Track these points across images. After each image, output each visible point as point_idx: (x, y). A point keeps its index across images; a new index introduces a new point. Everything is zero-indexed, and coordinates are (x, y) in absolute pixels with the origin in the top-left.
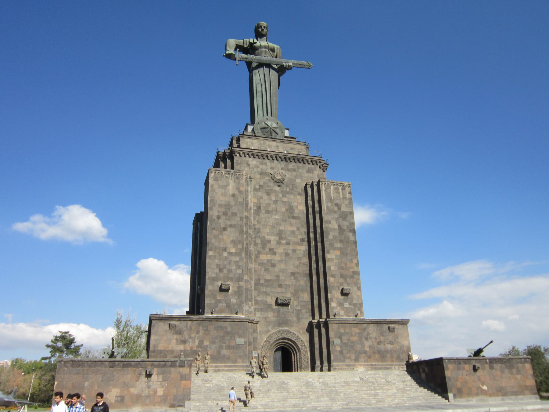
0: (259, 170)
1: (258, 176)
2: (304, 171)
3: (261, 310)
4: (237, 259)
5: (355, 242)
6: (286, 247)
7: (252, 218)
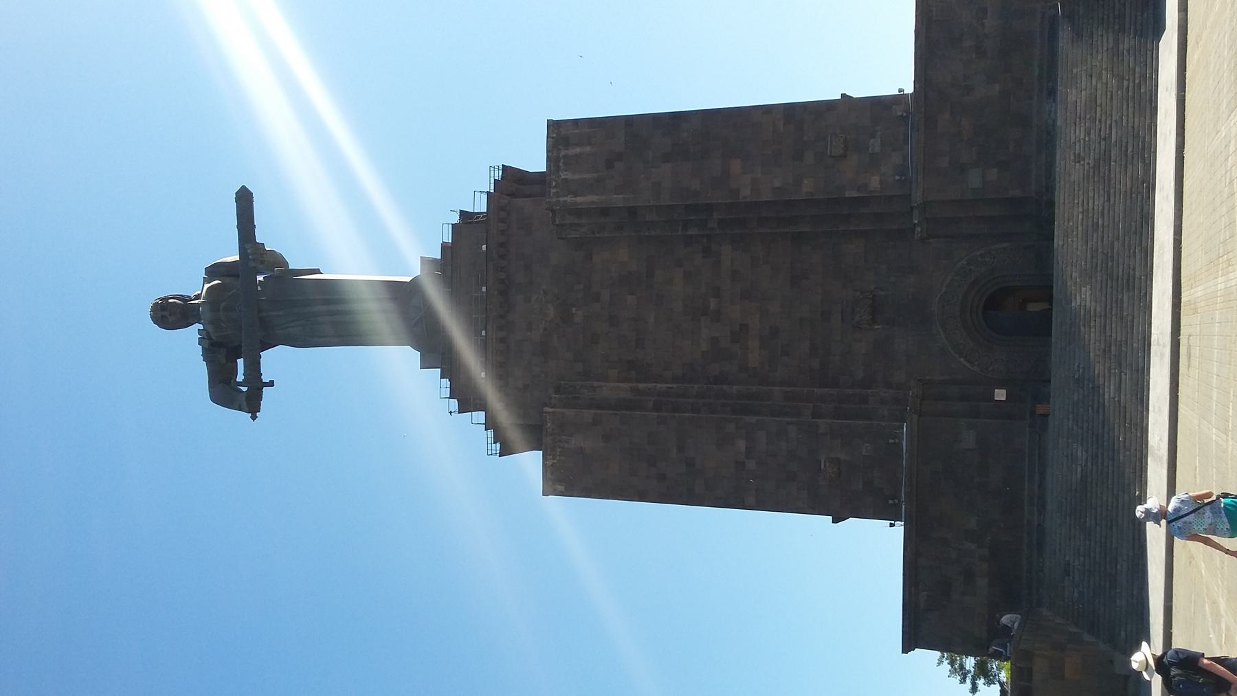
7: (661, 386)
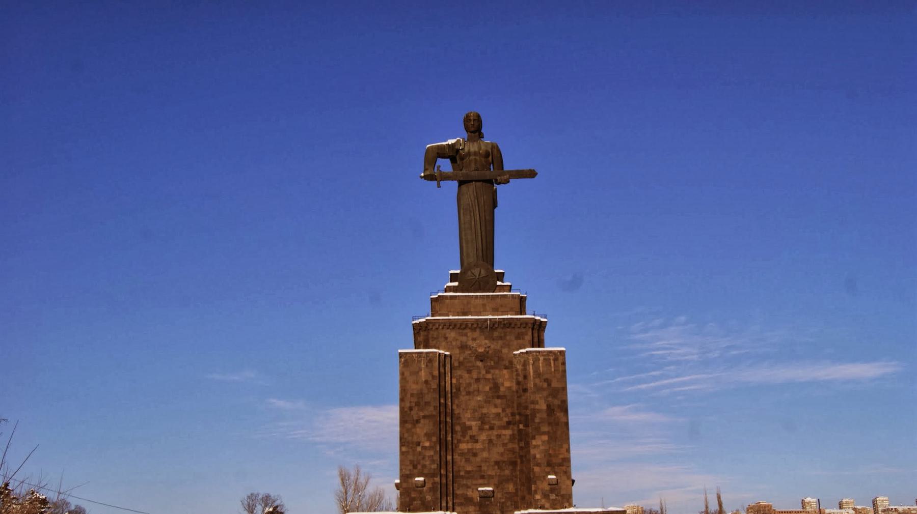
0: (459, 343)
1: (457, 351)
2: (513, 338)
3: (461, 504)
4: (432, 453)
5: (567, 424)
6: (490, 432)
